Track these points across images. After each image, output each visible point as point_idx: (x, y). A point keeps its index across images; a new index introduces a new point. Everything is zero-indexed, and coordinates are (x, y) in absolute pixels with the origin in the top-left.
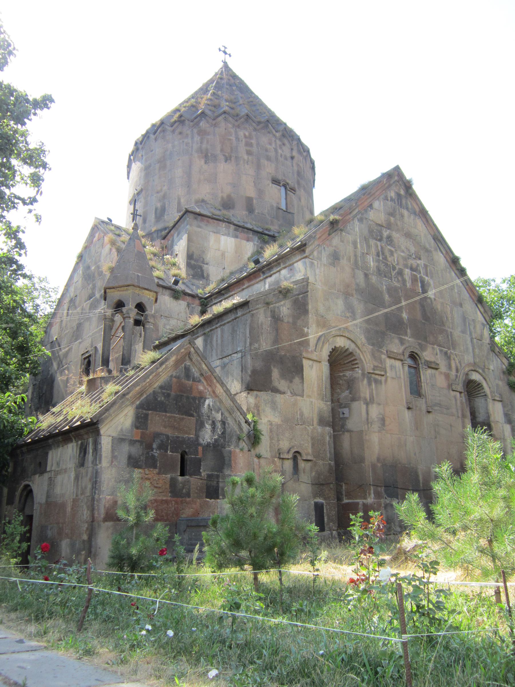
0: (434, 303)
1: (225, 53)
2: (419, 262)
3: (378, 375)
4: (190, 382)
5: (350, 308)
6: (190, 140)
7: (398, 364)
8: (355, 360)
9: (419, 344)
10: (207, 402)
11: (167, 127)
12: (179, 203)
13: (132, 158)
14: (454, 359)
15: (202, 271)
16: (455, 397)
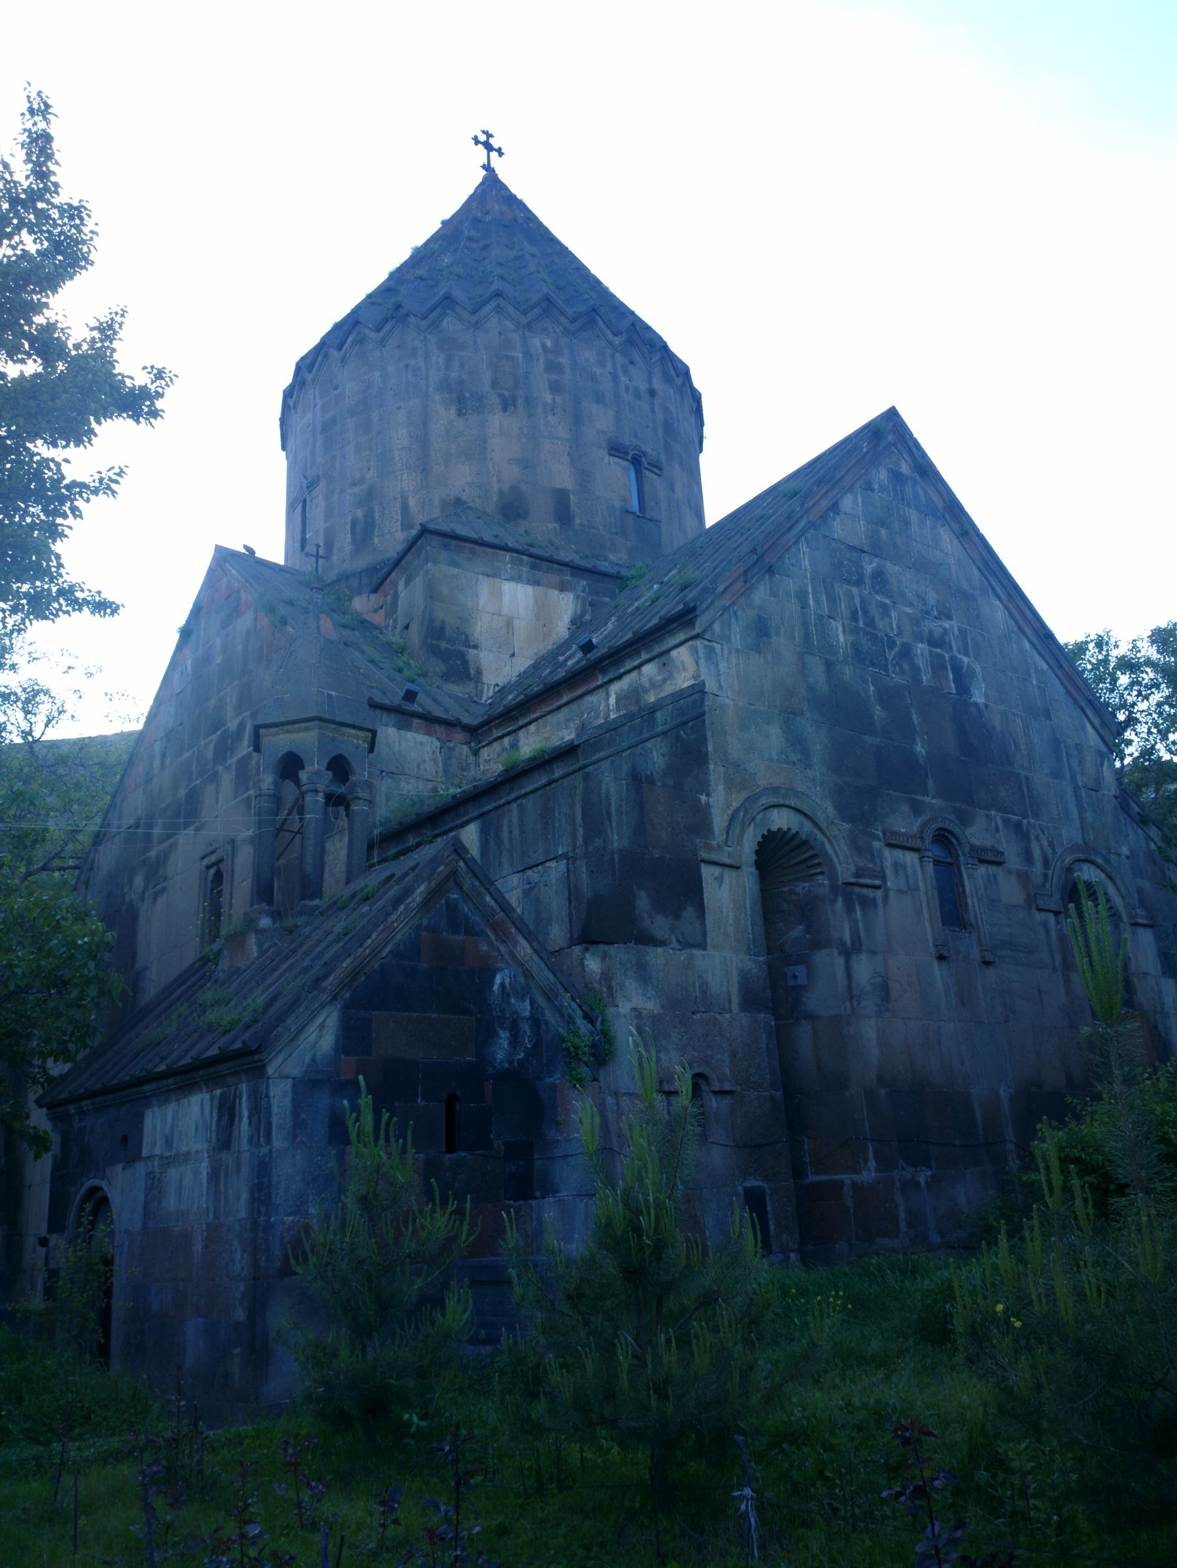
1: (488, 147)
2: (946, 624)
3: (867, 886)
4: (460, 938)
5: (797, 742)
6: (423, 365)
7: (910, 858)
8: (815, 856)
10: (498, 980)
11: (367, 331)
12: (405, 509)
13: (291, 402)
14: (1037, 838)
15: (466, 663)
16: (1045, 924)
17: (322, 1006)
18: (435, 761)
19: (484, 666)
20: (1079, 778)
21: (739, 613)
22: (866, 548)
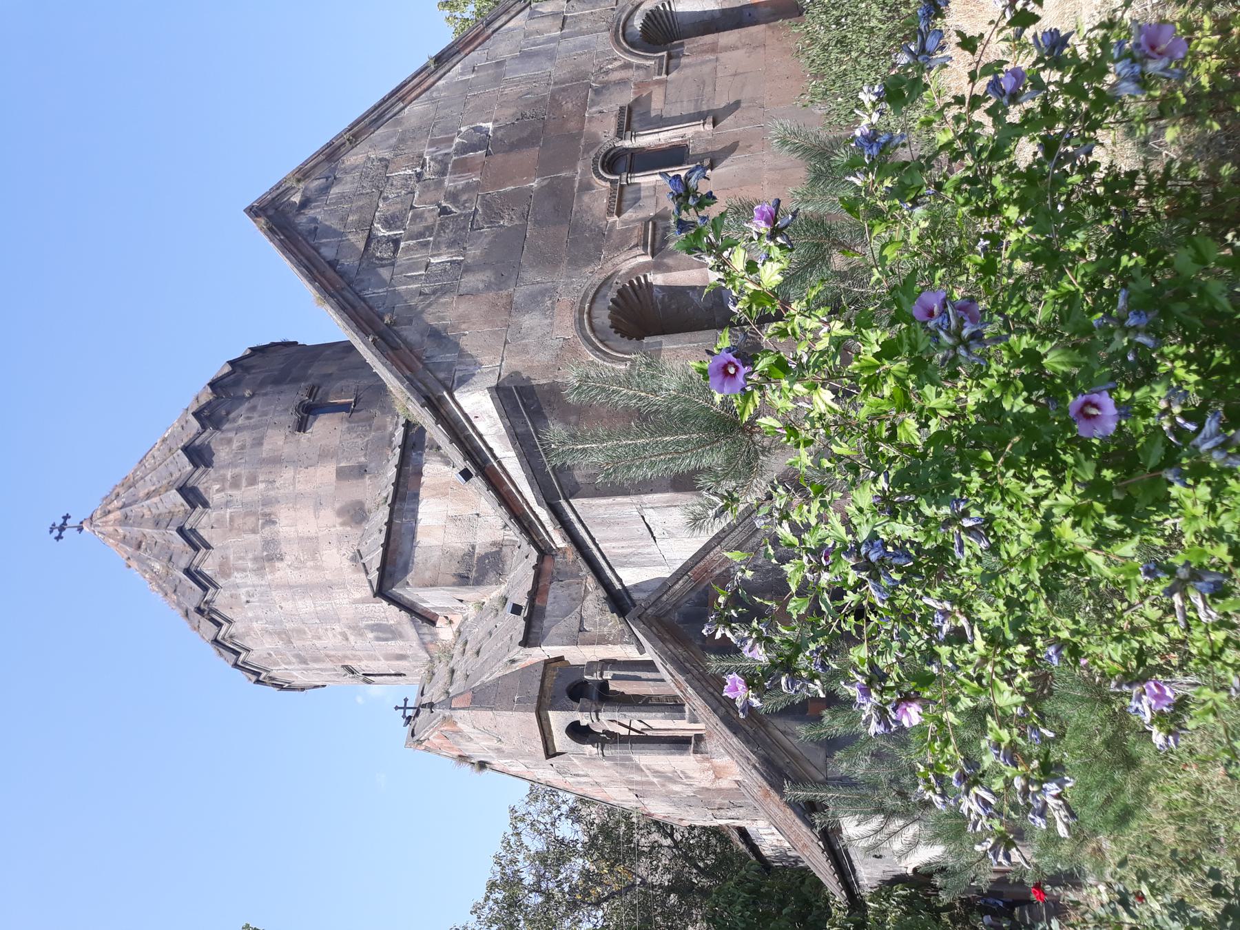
0: (502, 123)
3: (654, 235)
5: (534, 302)
6: (243, 591)
9: (587, 151)
12: (363, 601)
15: (487, 556)
17: (769, 734)
18: (569, 585)
19: (489, 540)
20: (553, 34)
21: (428, 354)
22: (366, 234)
